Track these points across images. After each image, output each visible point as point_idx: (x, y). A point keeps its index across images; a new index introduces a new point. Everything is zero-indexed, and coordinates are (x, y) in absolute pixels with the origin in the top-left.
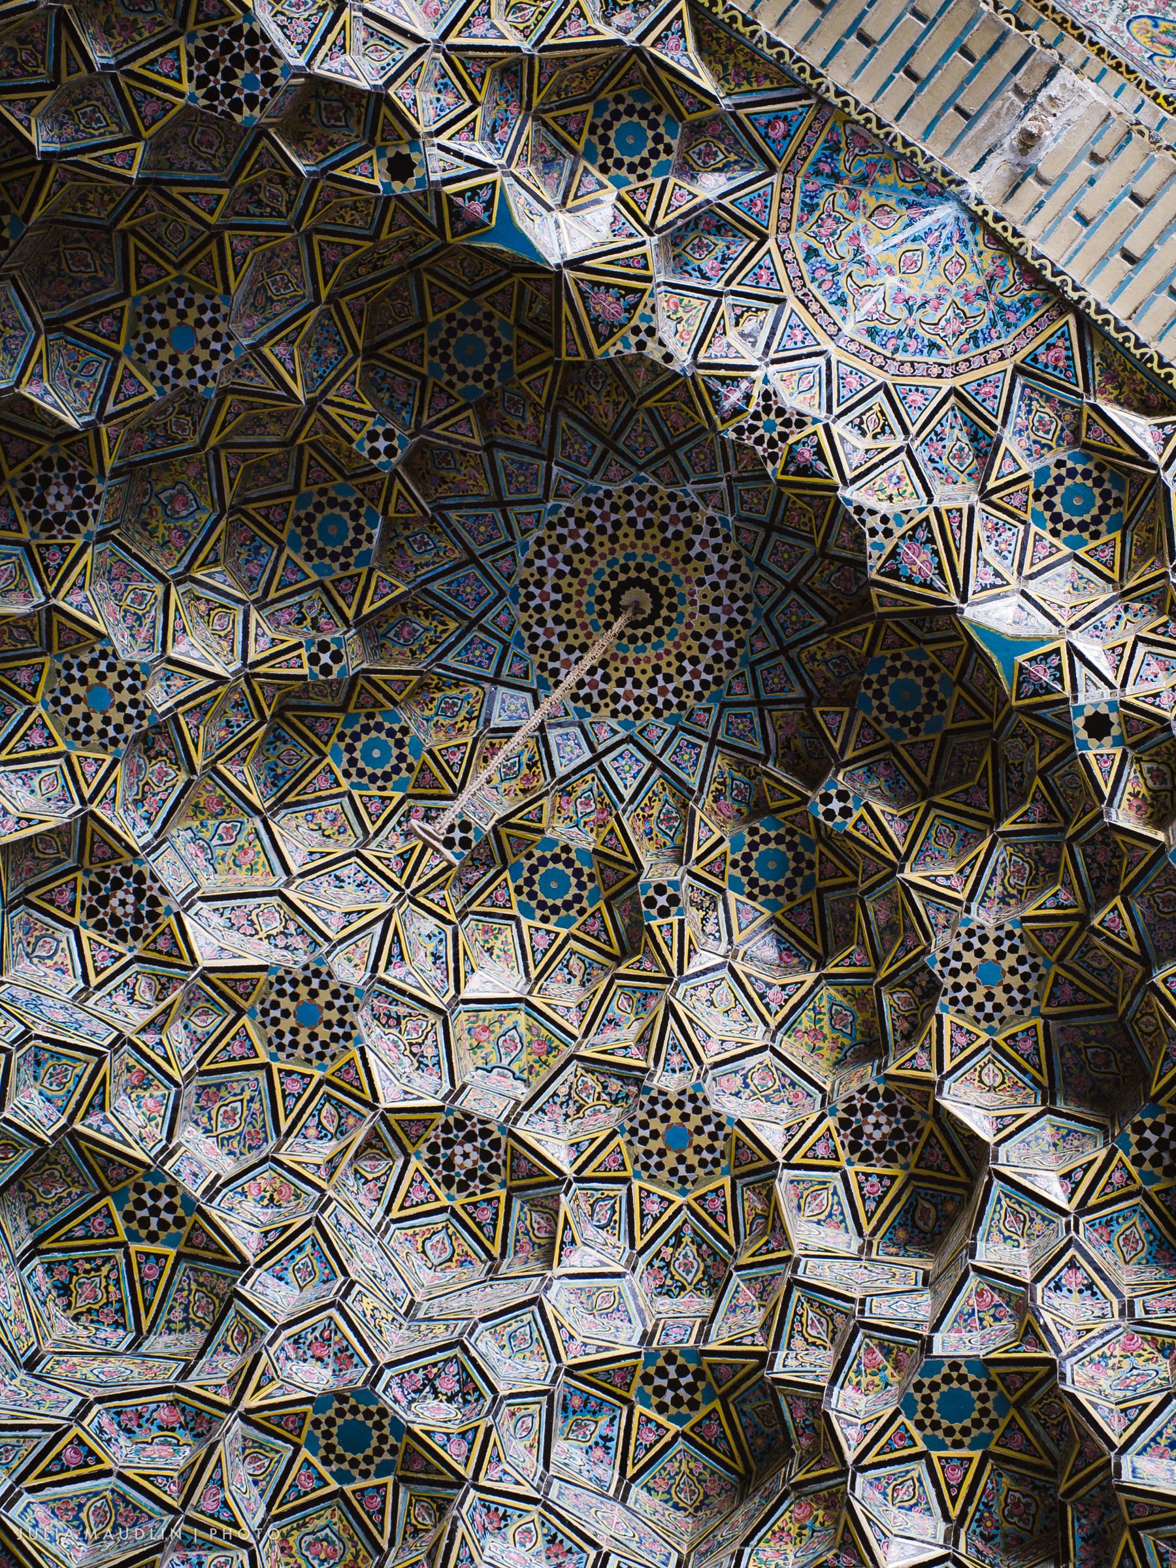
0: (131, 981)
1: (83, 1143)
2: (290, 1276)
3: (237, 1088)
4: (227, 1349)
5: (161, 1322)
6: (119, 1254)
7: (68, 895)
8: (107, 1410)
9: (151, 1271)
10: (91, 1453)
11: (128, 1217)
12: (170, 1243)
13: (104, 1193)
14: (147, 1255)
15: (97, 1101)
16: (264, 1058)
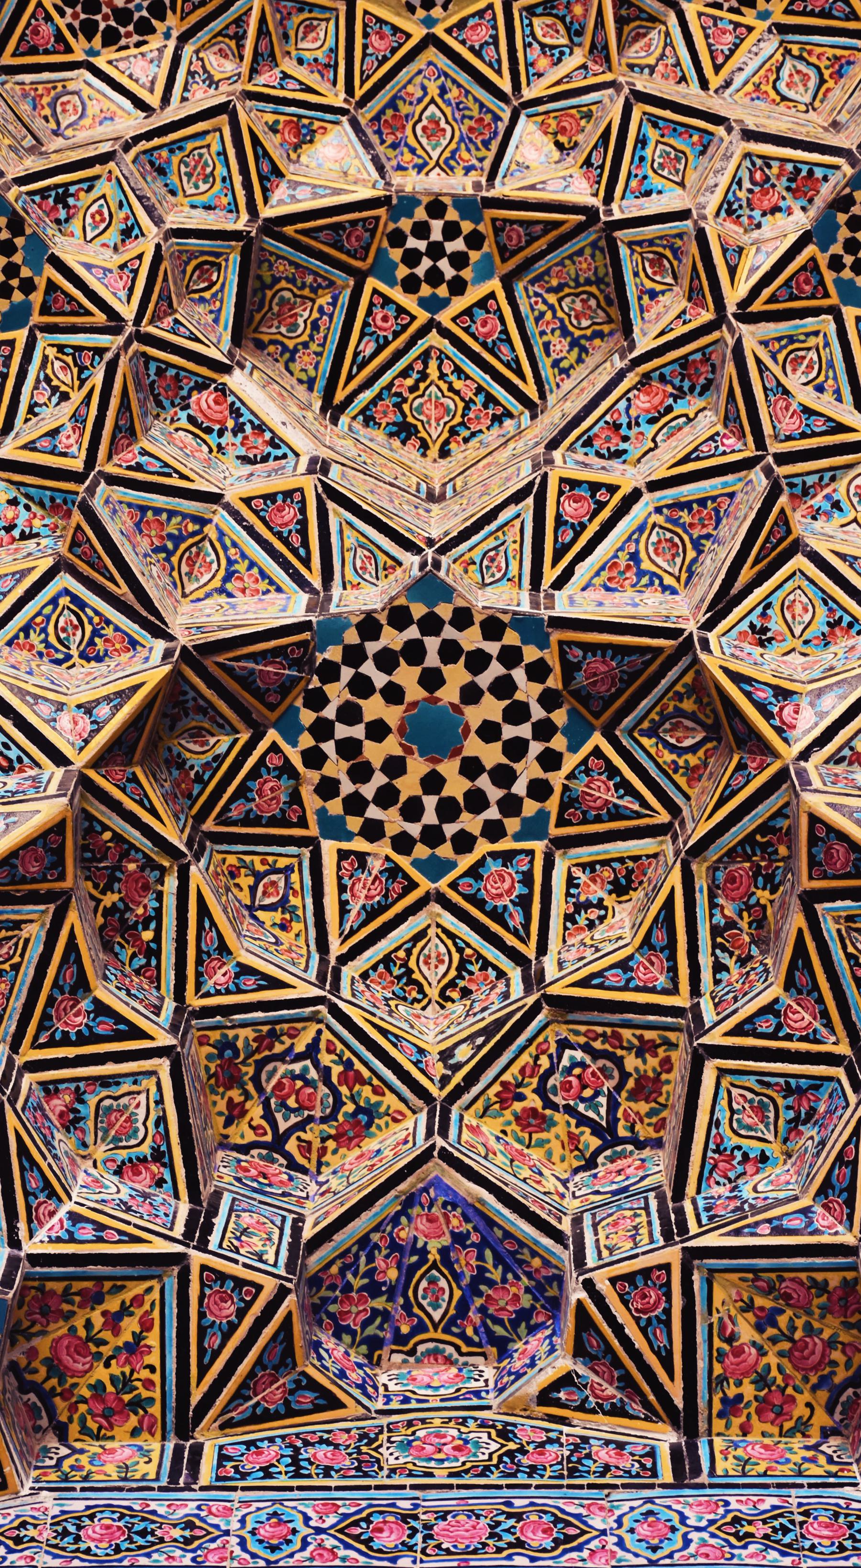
0: (196, 67)
1: (289, 230)
2: (656, 182)
3: (415, 90)
4: (653, 295)
5: (547, 372)
6: (434, 339)
7: (46, 29)
8: (571, 448)
9: (486, 326)
10: (595, 487)
11: (410, 285)
12: (485, 274)
13: (360, 277)
14: (468, 312)
15: (266, 167)
16: (418, 33)
